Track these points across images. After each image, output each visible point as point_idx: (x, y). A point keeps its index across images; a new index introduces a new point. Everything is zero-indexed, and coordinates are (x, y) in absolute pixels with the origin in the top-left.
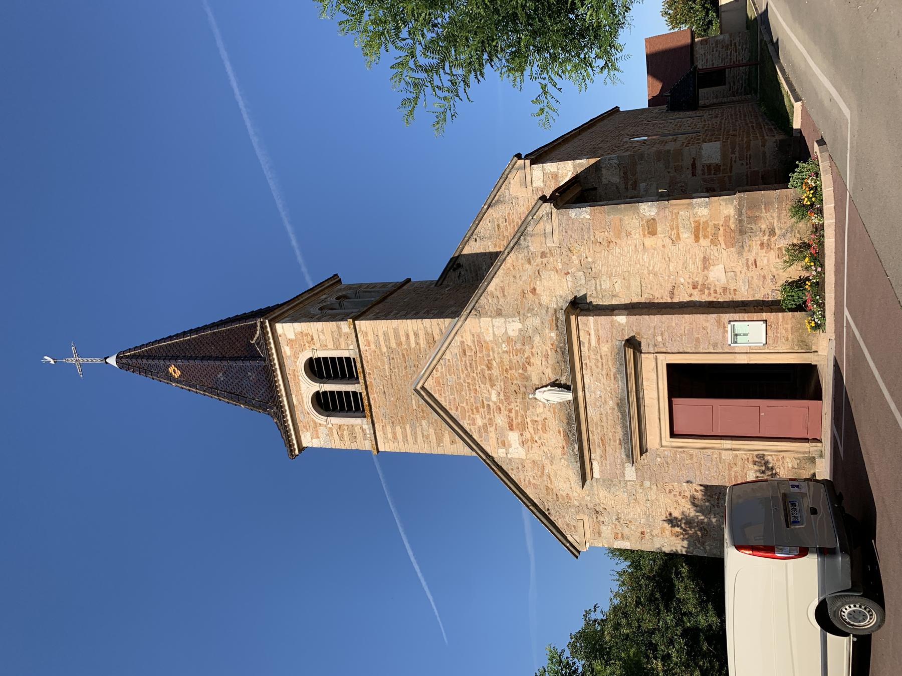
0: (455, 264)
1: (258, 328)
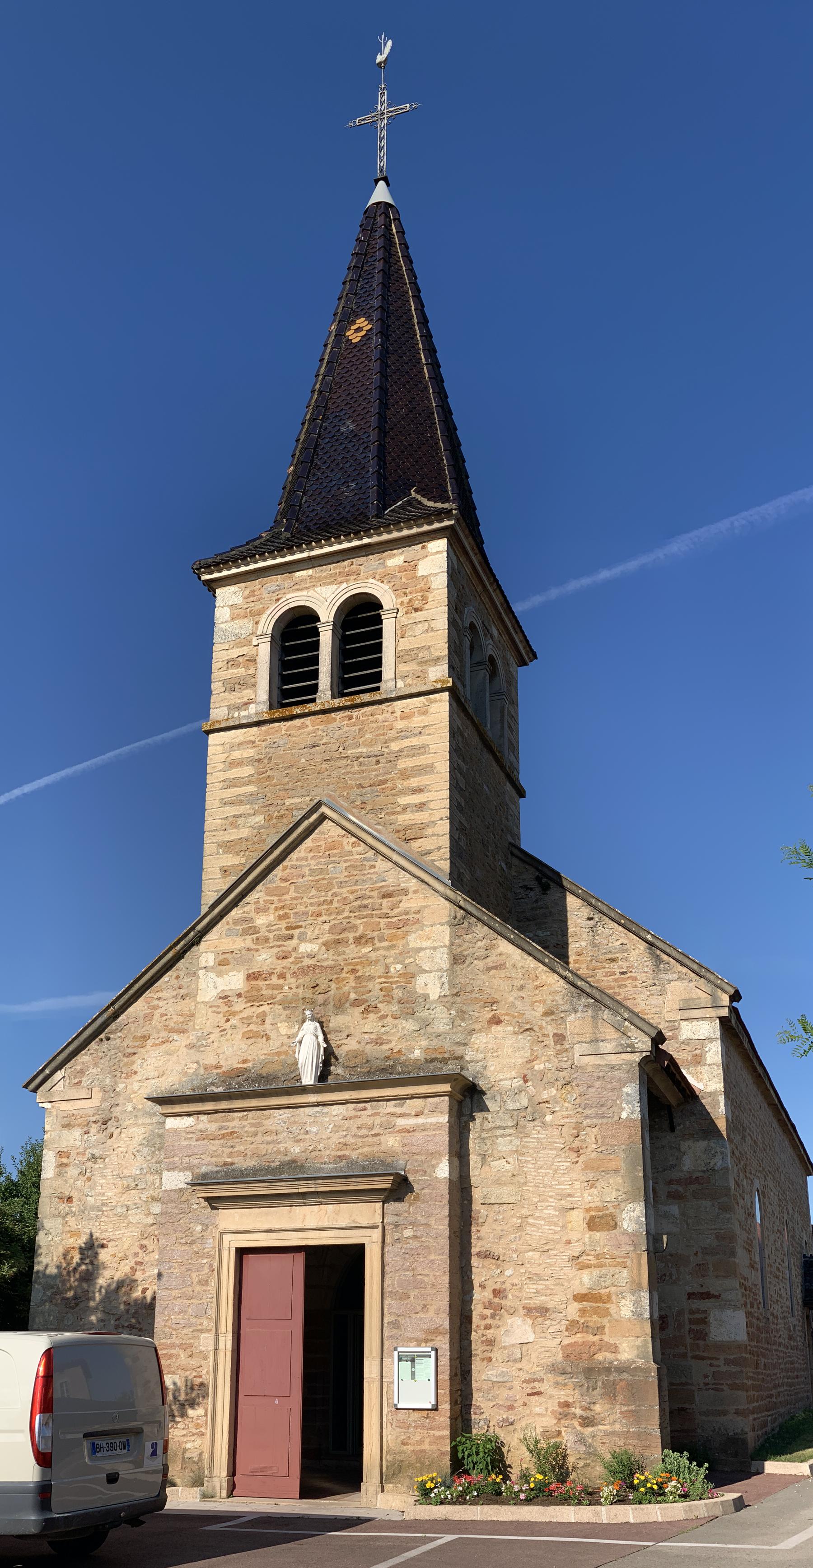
0: (549, 881)
1: (439, 505)
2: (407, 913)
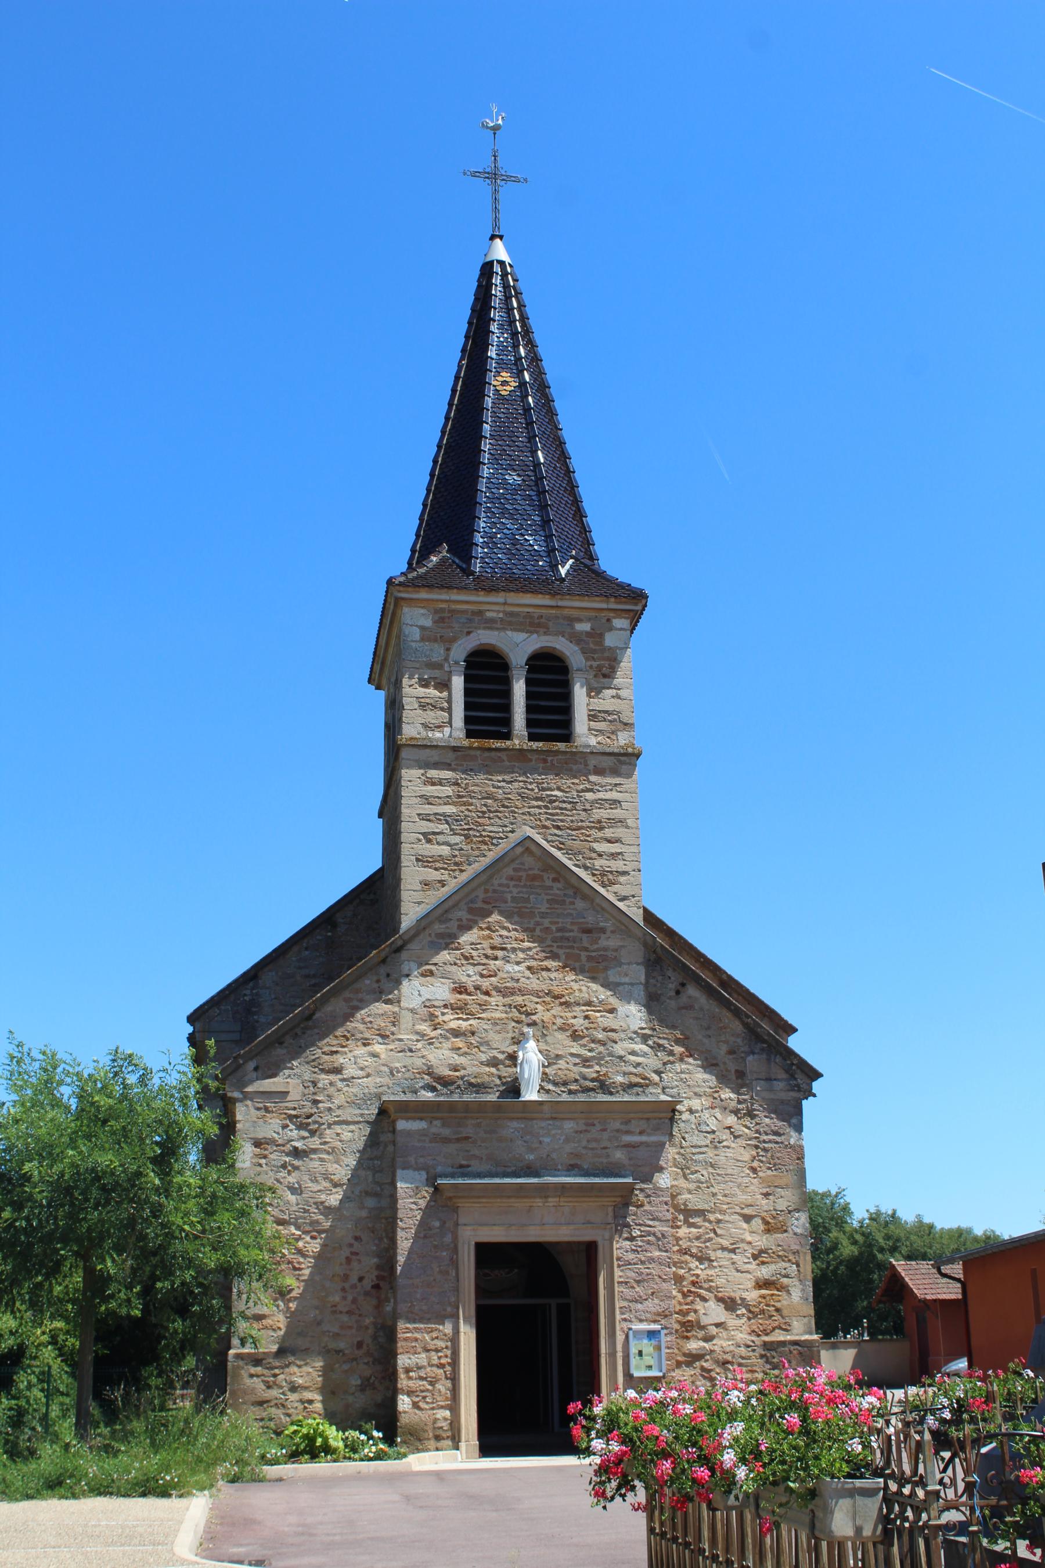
2: (605, 949)
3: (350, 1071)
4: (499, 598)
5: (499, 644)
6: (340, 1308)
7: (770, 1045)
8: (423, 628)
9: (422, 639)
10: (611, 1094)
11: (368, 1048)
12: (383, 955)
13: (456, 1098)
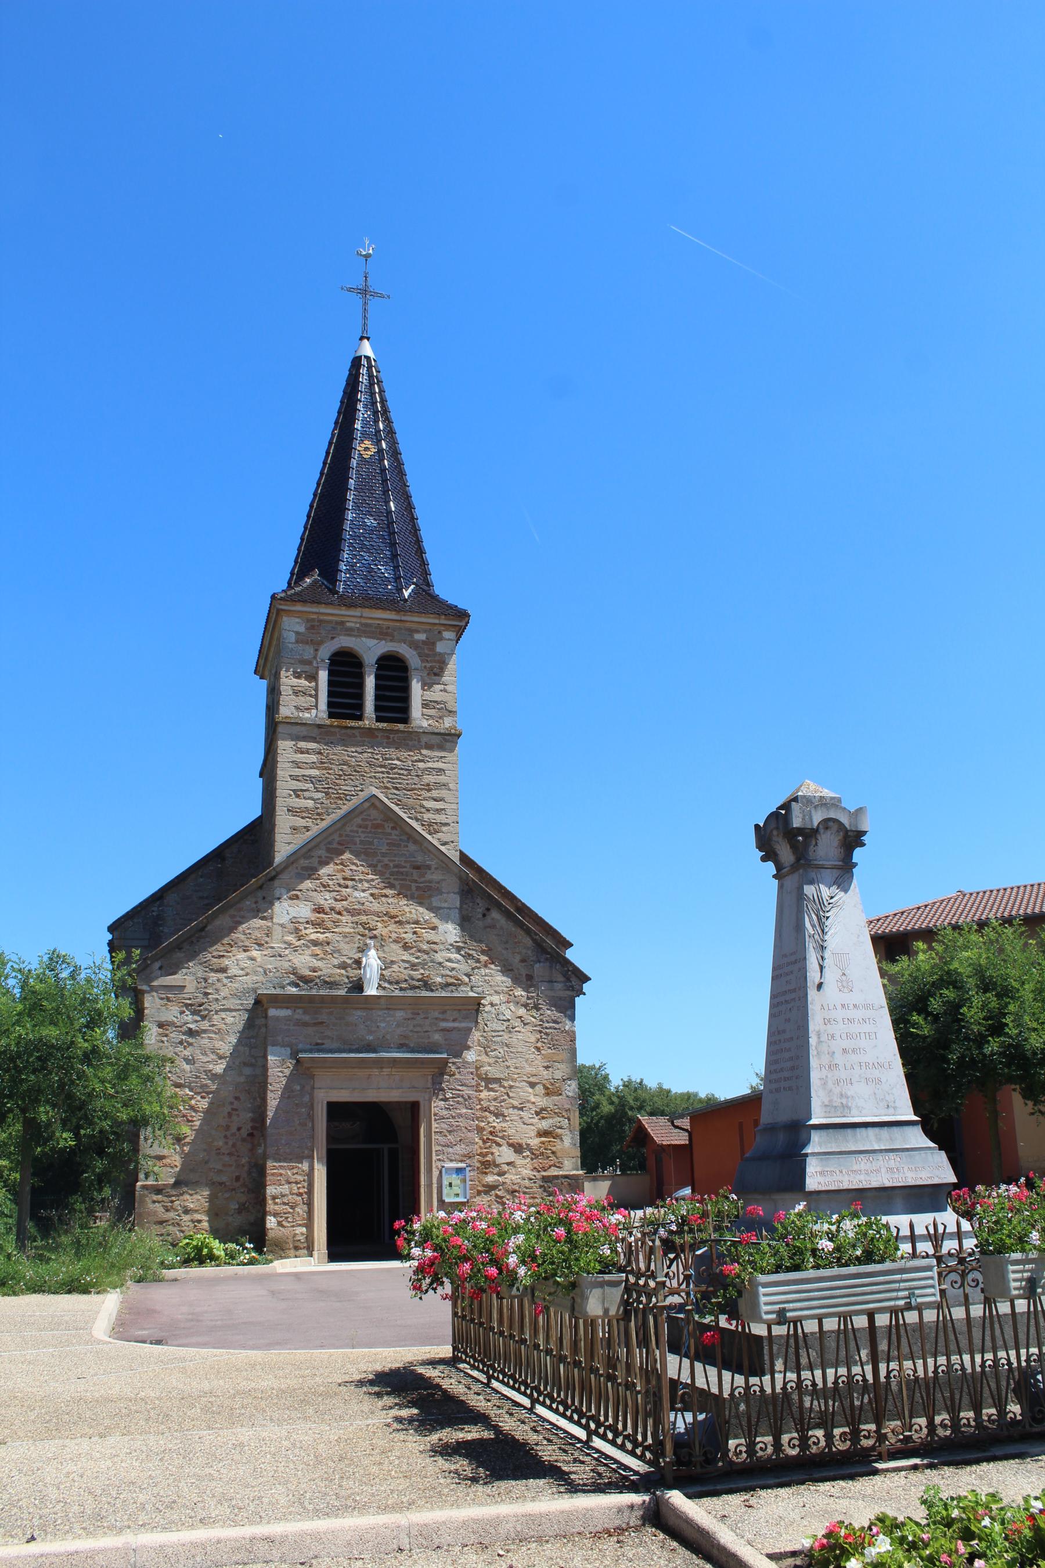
2: (430, 882)
3: (233, 971)
4: (357, 612)
5: (356, 648)
6: (222, 1151)
7: (552, 956)
8: (297, 633)
9: (297, 642)
10: (432, 991)
11: (248, 953)
12: (260, 882)
13: (314, 992)
